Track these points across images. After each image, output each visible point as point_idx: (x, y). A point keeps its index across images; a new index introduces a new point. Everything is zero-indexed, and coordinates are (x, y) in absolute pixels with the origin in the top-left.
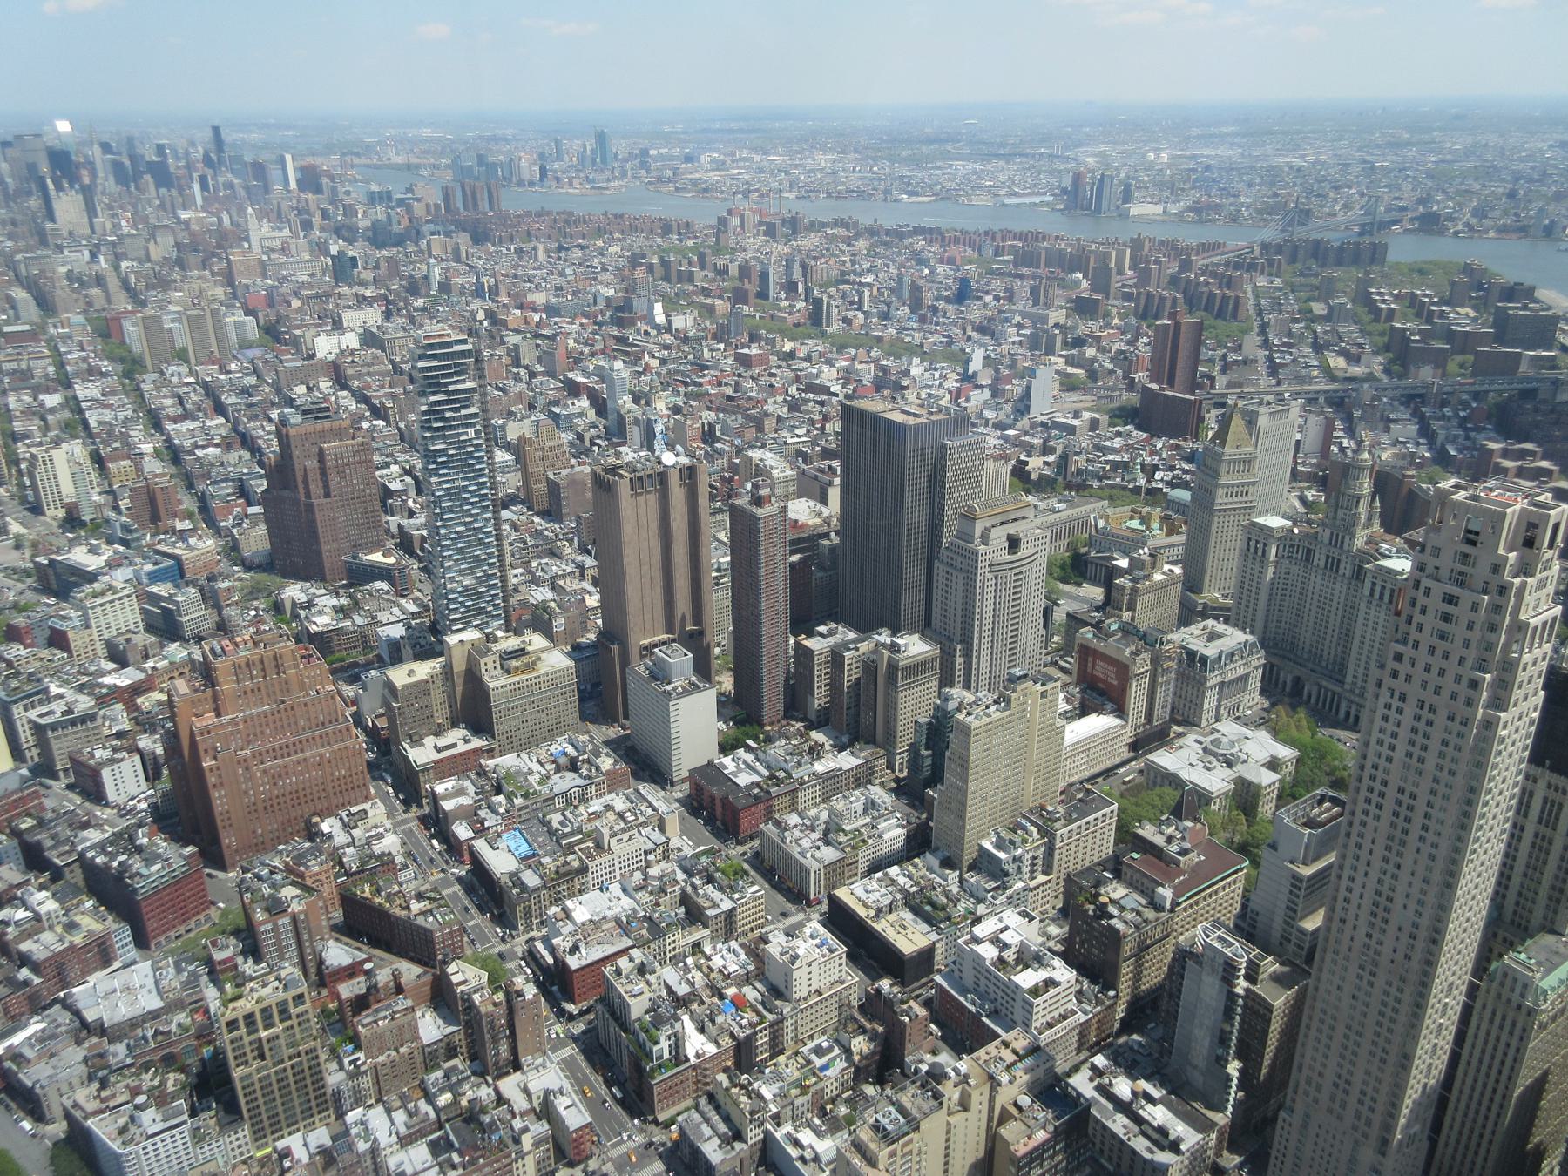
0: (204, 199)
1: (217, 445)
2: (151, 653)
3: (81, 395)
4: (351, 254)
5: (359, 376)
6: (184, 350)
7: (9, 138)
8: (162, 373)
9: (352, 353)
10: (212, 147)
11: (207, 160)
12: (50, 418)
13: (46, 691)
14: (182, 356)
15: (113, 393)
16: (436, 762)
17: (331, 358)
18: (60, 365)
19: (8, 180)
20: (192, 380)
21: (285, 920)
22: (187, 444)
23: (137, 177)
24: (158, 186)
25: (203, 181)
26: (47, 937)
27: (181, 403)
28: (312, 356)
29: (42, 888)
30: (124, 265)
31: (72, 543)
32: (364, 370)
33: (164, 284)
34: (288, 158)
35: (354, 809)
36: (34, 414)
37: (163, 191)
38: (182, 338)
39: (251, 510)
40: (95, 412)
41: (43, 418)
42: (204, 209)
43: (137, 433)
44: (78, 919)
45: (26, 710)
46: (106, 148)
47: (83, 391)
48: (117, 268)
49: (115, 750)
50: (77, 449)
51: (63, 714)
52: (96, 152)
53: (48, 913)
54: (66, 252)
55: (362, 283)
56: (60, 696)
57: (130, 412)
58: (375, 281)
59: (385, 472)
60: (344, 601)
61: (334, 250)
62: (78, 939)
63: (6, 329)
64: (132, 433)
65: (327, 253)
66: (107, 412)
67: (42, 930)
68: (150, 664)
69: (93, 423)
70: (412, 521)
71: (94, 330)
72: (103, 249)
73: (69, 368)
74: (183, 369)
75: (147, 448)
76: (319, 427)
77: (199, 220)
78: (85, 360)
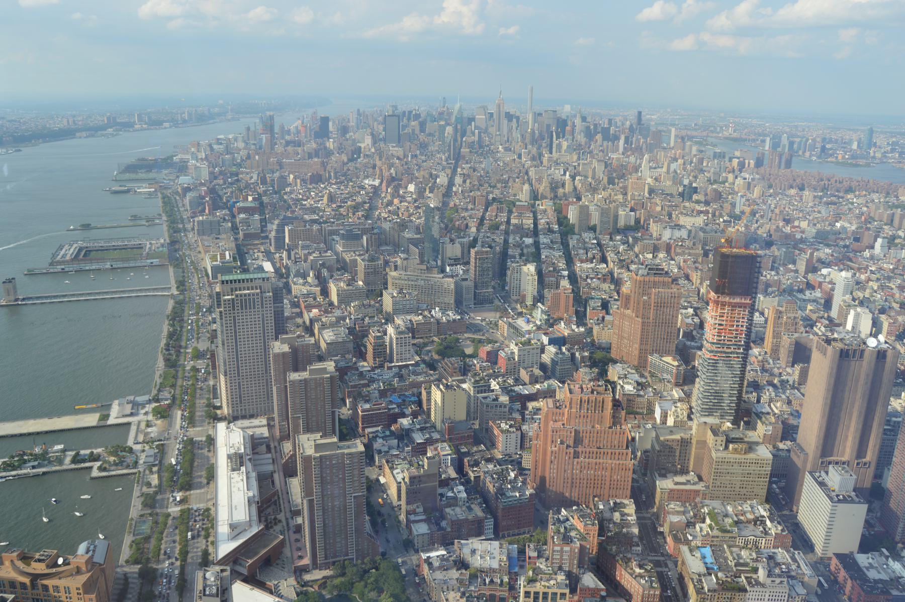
0: (625, 148)
1: (599, 279)
2: (539, 380)
3: (541, 242)
4: (694, 185)
5: (683, 254)
6: (595, 226)
7: (543, 112)
8: (581, 235)
9: (683, 240)
10: (635, 121)
11: (631, 129)
12: (525, 251)
13: (490, 386)
14: (593, 229)
15: (556, 243)
16: (672, 490)
17: (668, 241)
18: (536, 224)
19: (537, 132)
20: (595, 242)
21: (567, 548)
22: (584, 276)
23: (596, 133)
24: (603, 140)
25: (627, 139)
26: (458, 509)
27: (587, 253)
28: (660, 239)
29: (462, 484)
30: (578, 178)
31: (520, 314)
32: (687, 251)
33: (594, 190)
34: (673, 130)
35: (618, 501)
36: (518, 247)
37: (605, 143)
38: (595, 219)
39: (607, 318)
40: (546, 250)
41: (522, 250)
42: (623, 154)
43: (562, 265)
44: (472, 506)
45: (478, 393)
46: (584, 119)
47: (544, 240)
48: (573, 178)
49: (511, 426)
50: (531, 268)
51: (494, 400)
52: (578, 121)
53: (461, 498)
54: (553, 169)
55: (698, 202)
56: (493, 391)
57: (561, 253)
58: (707, 203)
59: (684, 311)
60: (644, 380)
61: (686, 182)
62: (470, 517)
63: (517, 203)
64: (560, 264)
65: (681, 183)
66: (551, 251)
67: (457, 506)
68: (538, 386)
69: (543, 257)
70: (693, 344)
71: (555, 210)
72: (570, 168)
73: (540, 227)
74: (592, 235)
75: (566, 273)
76: (657, 279)
77: (618, 159)
78: (548, 223)
